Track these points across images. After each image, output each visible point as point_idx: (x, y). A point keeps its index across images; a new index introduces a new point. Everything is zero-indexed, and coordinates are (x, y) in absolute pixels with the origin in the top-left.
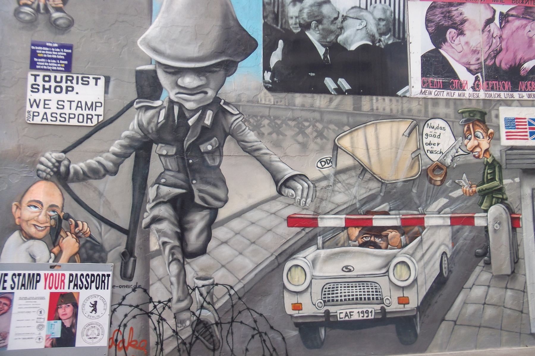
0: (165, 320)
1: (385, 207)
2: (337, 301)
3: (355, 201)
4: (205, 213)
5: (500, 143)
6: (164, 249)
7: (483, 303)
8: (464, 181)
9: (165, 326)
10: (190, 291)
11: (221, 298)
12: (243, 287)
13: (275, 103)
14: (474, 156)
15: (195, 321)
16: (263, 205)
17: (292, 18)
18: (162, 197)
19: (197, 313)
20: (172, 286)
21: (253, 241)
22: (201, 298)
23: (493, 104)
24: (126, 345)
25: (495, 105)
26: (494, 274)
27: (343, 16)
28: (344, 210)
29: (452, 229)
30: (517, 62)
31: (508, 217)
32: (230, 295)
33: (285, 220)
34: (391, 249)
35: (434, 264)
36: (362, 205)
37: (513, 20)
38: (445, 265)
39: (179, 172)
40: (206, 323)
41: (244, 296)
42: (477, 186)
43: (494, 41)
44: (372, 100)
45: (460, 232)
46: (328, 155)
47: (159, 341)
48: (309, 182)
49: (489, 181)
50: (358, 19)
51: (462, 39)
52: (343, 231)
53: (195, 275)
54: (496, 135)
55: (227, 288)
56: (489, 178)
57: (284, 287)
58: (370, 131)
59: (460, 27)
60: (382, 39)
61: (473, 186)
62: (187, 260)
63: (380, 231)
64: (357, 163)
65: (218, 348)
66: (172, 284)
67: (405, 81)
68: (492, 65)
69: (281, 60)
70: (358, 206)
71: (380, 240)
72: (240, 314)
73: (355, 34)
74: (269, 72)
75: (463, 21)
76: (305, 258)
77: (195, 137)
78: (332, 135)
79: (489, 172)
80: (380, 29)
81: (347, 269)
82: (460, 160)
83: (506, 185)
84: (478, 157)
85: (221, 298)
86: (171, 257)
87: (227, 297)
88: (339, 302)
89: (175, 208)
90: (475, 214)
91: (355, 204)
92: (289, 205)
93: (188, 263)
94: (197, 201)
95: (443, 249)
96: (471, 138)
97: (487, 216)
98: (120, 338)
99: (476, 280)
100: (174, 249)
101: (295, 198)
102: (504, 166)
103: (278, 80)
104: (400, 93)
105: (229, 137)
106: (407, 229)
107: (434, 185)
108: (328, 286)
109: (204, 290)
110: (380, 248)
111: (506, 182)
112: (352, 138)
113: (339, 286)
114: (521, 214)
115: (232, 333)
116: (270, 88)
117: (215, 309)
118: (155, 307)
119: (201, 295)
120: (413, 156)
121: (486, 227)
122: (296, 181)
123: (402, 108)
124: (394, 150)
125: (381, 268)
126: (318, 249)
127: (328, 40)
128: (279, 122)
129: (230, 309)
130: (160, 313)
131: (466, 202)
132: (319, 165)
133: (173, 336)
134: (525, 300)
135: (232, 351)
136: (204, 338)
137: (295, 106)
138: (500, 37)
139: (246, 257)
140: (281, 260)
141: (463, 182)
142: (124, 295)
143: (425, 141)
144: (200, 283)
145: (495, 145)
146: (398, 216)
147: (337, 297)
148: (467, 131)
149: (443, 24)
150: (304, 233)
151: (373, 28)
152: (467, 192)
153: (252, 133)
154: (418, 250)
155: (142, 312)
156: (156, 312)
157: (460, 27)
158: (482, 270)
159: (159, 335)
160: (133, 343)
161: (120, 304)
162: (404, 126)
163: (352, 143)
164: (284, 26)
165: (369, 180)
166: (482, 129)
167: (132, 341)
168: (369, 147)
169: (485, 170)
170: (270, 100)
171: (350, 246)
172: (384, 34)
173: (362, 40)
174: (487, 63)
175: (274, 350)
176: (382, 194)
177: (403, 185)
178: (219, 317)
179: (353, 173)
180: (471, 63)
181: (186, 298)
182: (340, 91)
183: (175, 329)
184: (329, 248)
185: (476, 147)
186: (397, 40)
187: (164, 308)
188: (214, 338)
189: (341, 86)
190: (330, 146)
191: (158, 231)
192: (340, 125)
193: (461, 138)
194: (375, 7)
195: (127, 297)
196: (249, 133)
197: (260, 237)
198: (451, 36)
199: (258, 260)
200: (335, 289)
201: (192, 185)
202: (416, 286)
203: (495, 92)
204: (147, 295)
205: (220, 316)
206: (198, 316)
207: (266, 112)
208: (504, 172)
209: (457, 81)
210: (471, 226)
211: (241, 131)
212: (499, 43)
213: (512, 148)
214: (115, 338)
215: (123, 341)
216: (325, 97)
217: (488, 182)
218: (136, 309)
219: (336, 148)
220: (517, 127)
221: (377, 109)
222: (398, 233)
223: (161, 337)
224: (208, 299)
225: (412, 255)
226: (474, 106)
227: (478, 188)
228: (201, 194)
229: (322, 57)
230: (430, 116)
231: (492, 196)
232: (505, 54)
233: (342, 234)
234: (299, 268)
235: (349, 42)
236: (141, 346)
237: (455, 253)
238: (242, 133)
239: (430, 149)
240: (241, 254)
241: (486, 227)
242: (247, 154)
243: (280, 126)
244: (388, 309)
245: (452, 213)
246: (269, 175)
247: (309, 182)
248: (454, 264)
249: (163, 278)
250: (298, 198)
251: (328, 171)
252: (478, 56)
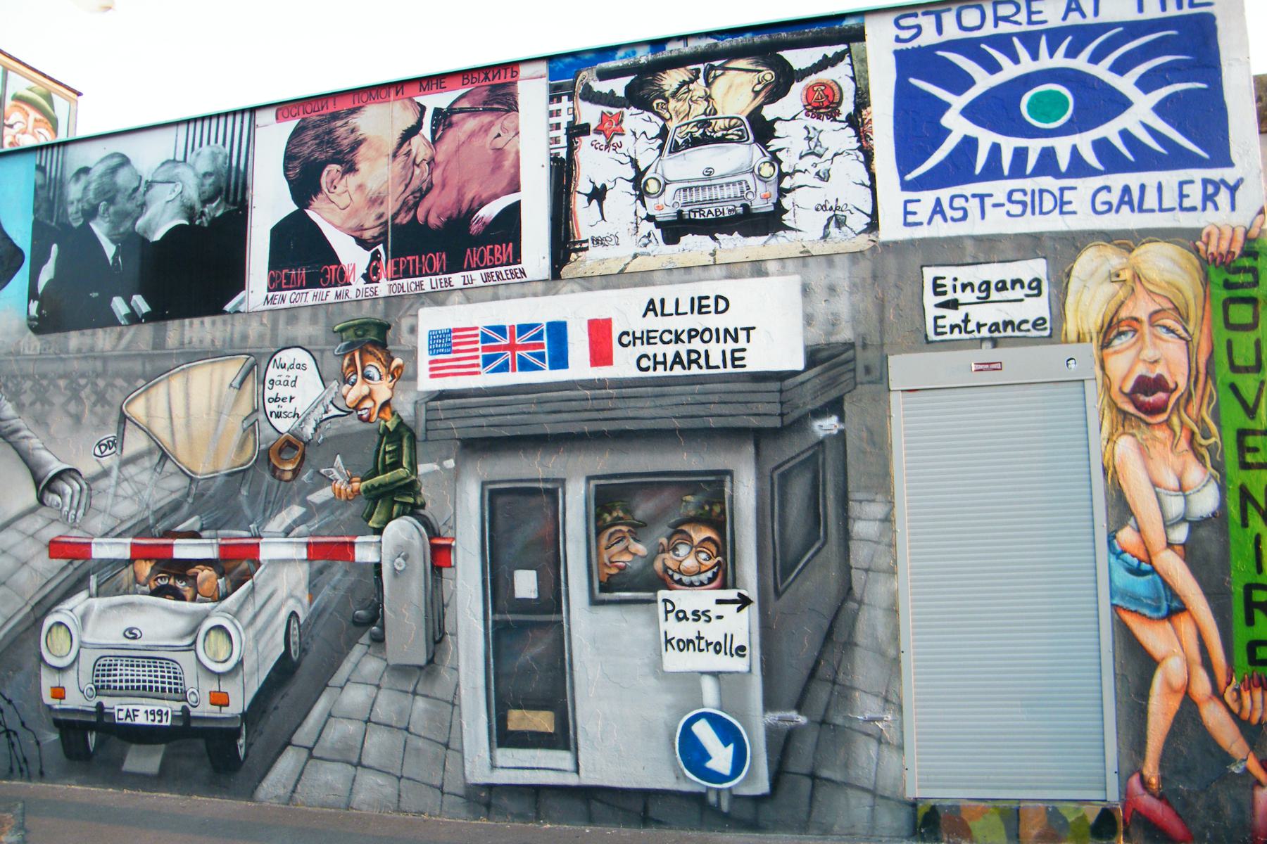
1: (193, 523)
2: (115, 688)
3: (146, 514)
5: (416, 385)
7: (366, 719)
8: (338, 469)
14: (360, 417)
17: (72, 203)
23: (407, 303)
25: (411, 306)
26: (392, 662)
27: (147, 182)
28: (129, 528)
29: (311, 567)
30: (465, 206)
31: (424, 546)
33: (46, 546)
34: (201, 601)
35: (273, 635)
36: (157, 521)
37: (463, 119)
38: (294, 638)
42: (363, 480)
43: (417, 171)
44: (183, 326)
45: (325, 573)
46: (111, 434)
48: (83, 482)
49: (386, 469)
50: (169, 182)
51: (352, 180)
52: (127, 566)
54: (408, 370)
56: (388, 461)
57: (42, 659)
58: (177, 383)
59: (349, 157)
60: (206, 210)
61: (354, 479)
63: (184, 568)
64: (153, 444)
67: (236, 281)
68: (409, 222)
70: (151, 521)
71: (184, 584)
73: (164, 211)
75: (357, 144)
76: (71, 611)
78: (119, 398)
79: (388, 448)
80: (204, 192)
81: (131, 634)
82: (331, 428)
83: (425, 475)
84: (368, 420)
88: (118, 692)
90: (356, 537)
91: (147, 518)
92: (53, 521)
95: (291, 605)
96: (356, 380)
97: (380, 542)
99: (353, 671)
101: (61, 510)
102: (420, 433)
104: (228, 307)
106: (231, 565)
107: (280, 479)
108: (102, 662)
110: (183, 598)
111: (423, 468)
112: (148, 400)
113: (119, 663)
114: (454, 539)
116: (36, 327)
120: (245, 426)
121: (378, 566)
122: (62, 479)
123: (232, 334)
124: (213, 416)
125: (182, 637)
126: (91, 596)
127: (122, 230)
128: (45, 382)
131: (338, 513)
132: (98, 452)
134: (454, 722)
137: (67, 352)
138: (432, 162)
140: (39, 613)
141: (335, 473)
143: (269, 394)
145: (404, 391)
146: (214, 541)
147: (115, 681)
148: (349, 366)
149: (316, 159)
150: (71, 568)
151: (192, 194)
152: (343, 492)
154: (246, 606)
157: (349, 157)
158: (366, 653)
162: (232, 369)
163: (148, 408)
165: (172, 474)
166: (379, 359)
168: (174, 415)
169: (380, 445)
170: (35, 347)
171: (137, 593)
172: (210, 200)
173: (173, 219)
174: (398, 221)
175: (25, 760)
176: (190, 500)
177: (227, 482)
179: (146, 462)
180: (366, 227)
182: (134, 318)
184: (107, 594)
185: (365, 398)
186: (232, 208)
189: (136, 309)
190: (115, 417)
192: (130, 378)
193: (335, 382)
194: (198, 154)
197: (12, 575)
198: (329, 180)
200: (113, 667)
202: (241, 673)
203: (410, 280)
207: (30, 368)
208: (420, 448)
209: (333, 267)
210: (347, 563)
212: (426, 174)
213: (442, 395)
216: (112, 331)
217: (385, 471)
219: (124, 419)
220: (454, 348)
221: (190, 342)
222: (213, 573)
225: (236, 614)
226: (366, 312)
227: (364, 483)
229: (111, 262)
230: (282, 345)
231: (392, 499)
232: (439, 195)
233: (125, 571)
234: (63, 627)
235: (153, 227)
237: (317, 615)
239: (277, 410)
241: (378, 566)
243: (46, 391)
244: (194, 712)
245: (311, 535)
246: (28, 472)
247: (83, 482)
248: (312, 637)
250: (66, 508)
251: (109, 461)
252: (381, 210)
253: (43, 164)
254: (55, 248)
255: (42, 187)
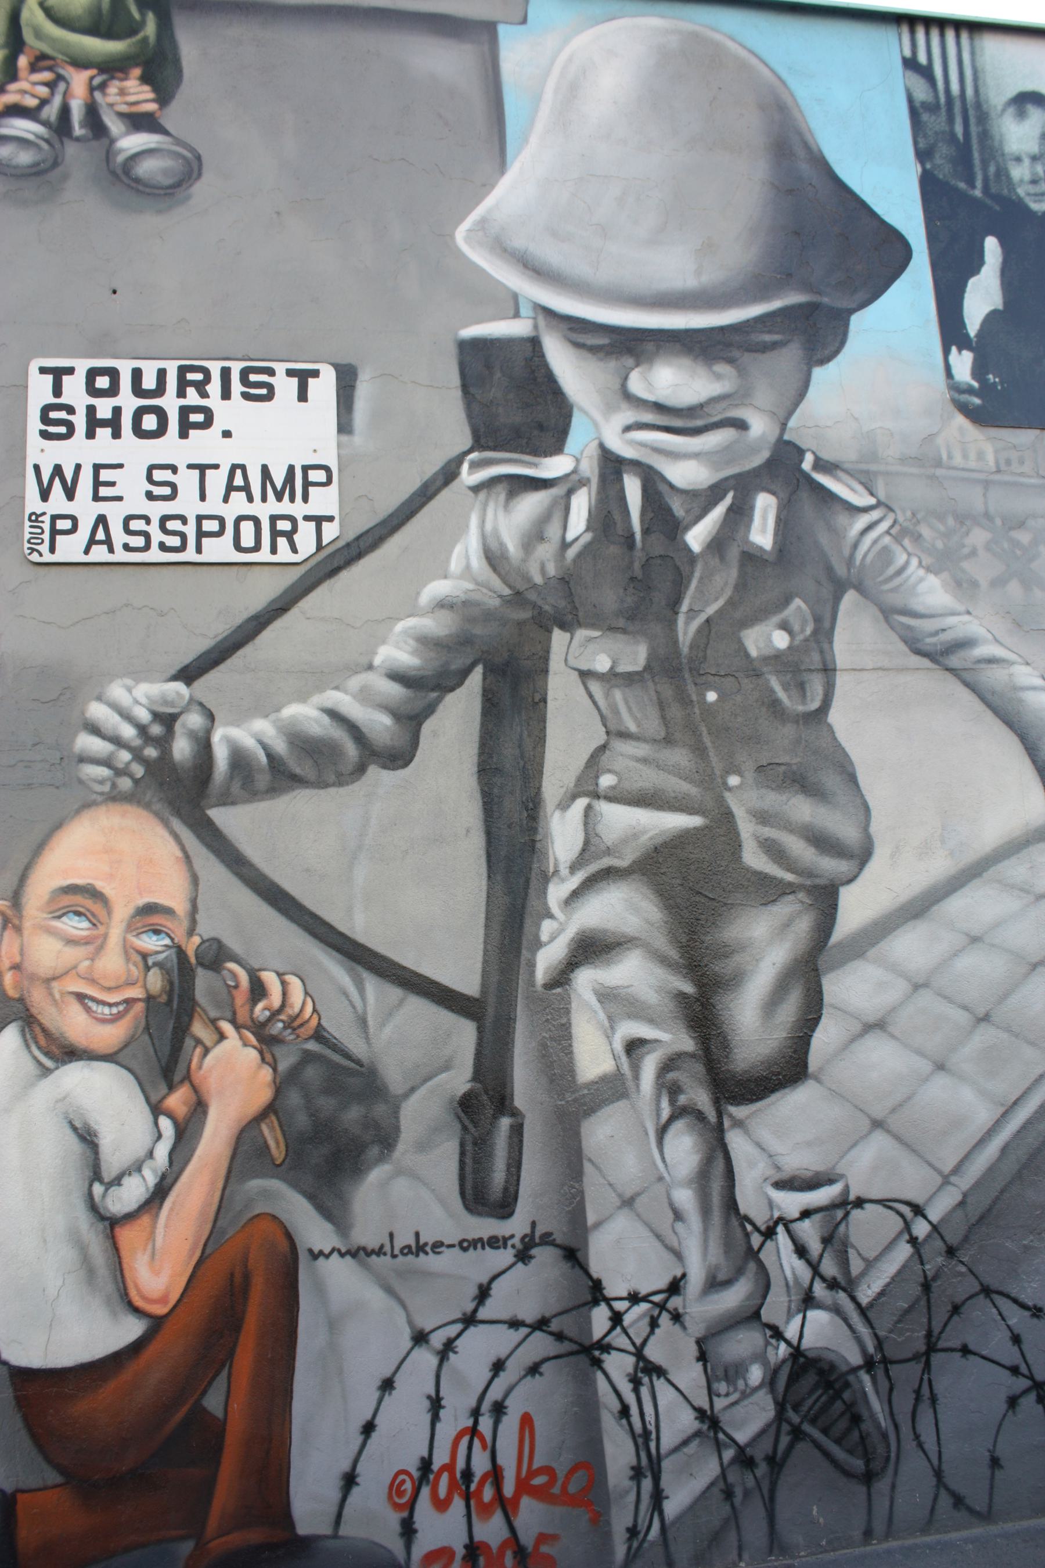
0: (659, 1371)
4: (785, 908)
6: (636, 1069)
9: (665, 1394)
10: (756, 1240)
11: (877, 1258)
12: (962, 1204)
13: (1003, 467)
15: (784, 1361)
16: (1006, 863)
18: (608, 852)
19: (791, 1331)
20: (679, 1226)
21: (981, 1011)
22: (800, 1266)
24: (509, 1489)
32: (913, 1241)
39: (668, 741)
40: (826, 1367)
41: (966, 1239)
47: (644, 1461)
53: (770, 1172)
55: (902, 1216)
62: (732, 1109)
65: (884, 1468)
66: (678, 1216)
69: (1000, 307)
72: (956, 1318)
74: (965, 352)
77: (717, 599)
85: (877, 1258)
86: (665, 1104)
87: (904, 1251)
89: (665, 896)
93: (738, 1124)
94: (753, 858)
98: (481, 1464)
100: (678, 1069)
103: (1001, 383)
105: (850, 598)
109: (809, 1231)
115: (933, 1400)
116: (977, 408)
117: (858, 1305)
118: (617, 1319)
119: (801, 1251)
129: (917, 1300)
130: (638, 1342)
133: (698, 1434)
135: (938, 1474)
136: (825, 1431)
139: (962, 1077)
142: (484, 1280)
144: (791, 1203)
153: (933, 581)
155: (566, 1347)
156: (622, 1341)
159: (643, 1439)
160: (539, 1480)
161: (469, 1320)
164: (993, 191)
167: (532, 1474)
170: (981, 456)
178: (876, 1335)
181: (740, 1272)
183: (706, 1406)
187: (654, 1324)
188: (864, 1426)
191: (606, 996)
195: (495, 1285)
196: (921, 580)
199: (1007, 1087)
201: (727, 795)
204: (578, 1271)
205: (882, 1333)
206: (795, 1342)
207: (974, 499)
211: (891, 570)
214: (461, 1464)
215: (496, 1474)
218: (538, 1334)
223: (653, 1445)
224: (829, 1268)
228: (768, 832)
236: (572, 1489)
238: (897, 581)
240: (940, 1067)
242: (926, 662)
246: (1015, 739)
249: (638, 1194)
253: (922, 59)
254: (991, 245)
255: (933, 108)
